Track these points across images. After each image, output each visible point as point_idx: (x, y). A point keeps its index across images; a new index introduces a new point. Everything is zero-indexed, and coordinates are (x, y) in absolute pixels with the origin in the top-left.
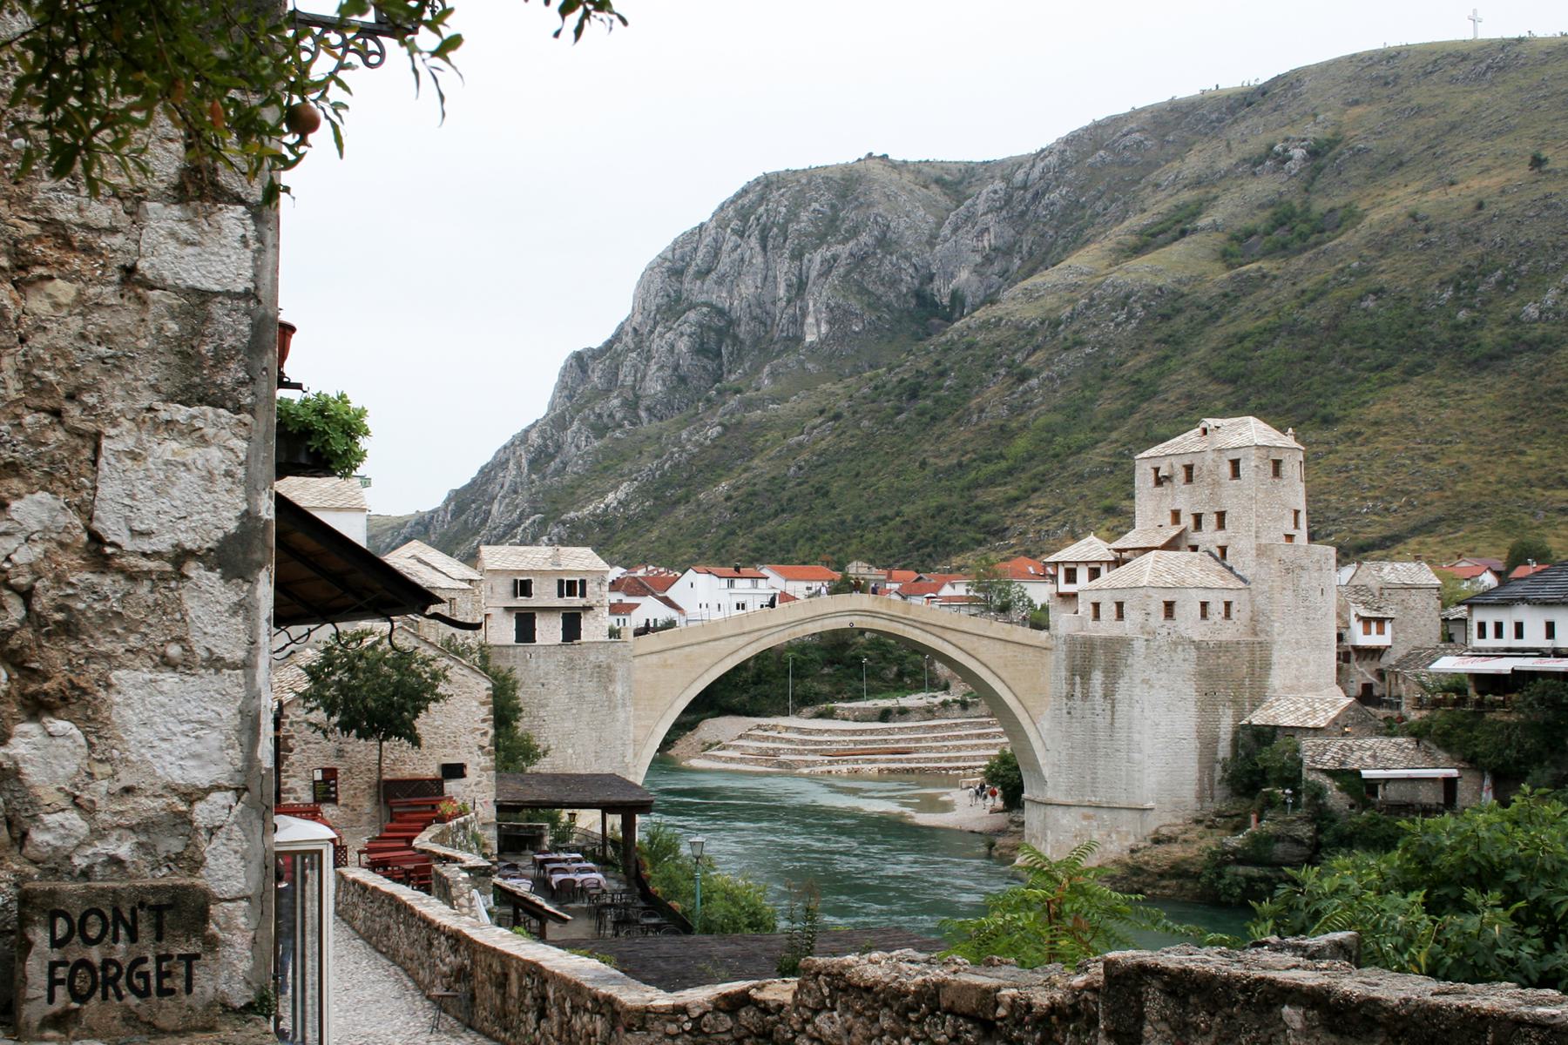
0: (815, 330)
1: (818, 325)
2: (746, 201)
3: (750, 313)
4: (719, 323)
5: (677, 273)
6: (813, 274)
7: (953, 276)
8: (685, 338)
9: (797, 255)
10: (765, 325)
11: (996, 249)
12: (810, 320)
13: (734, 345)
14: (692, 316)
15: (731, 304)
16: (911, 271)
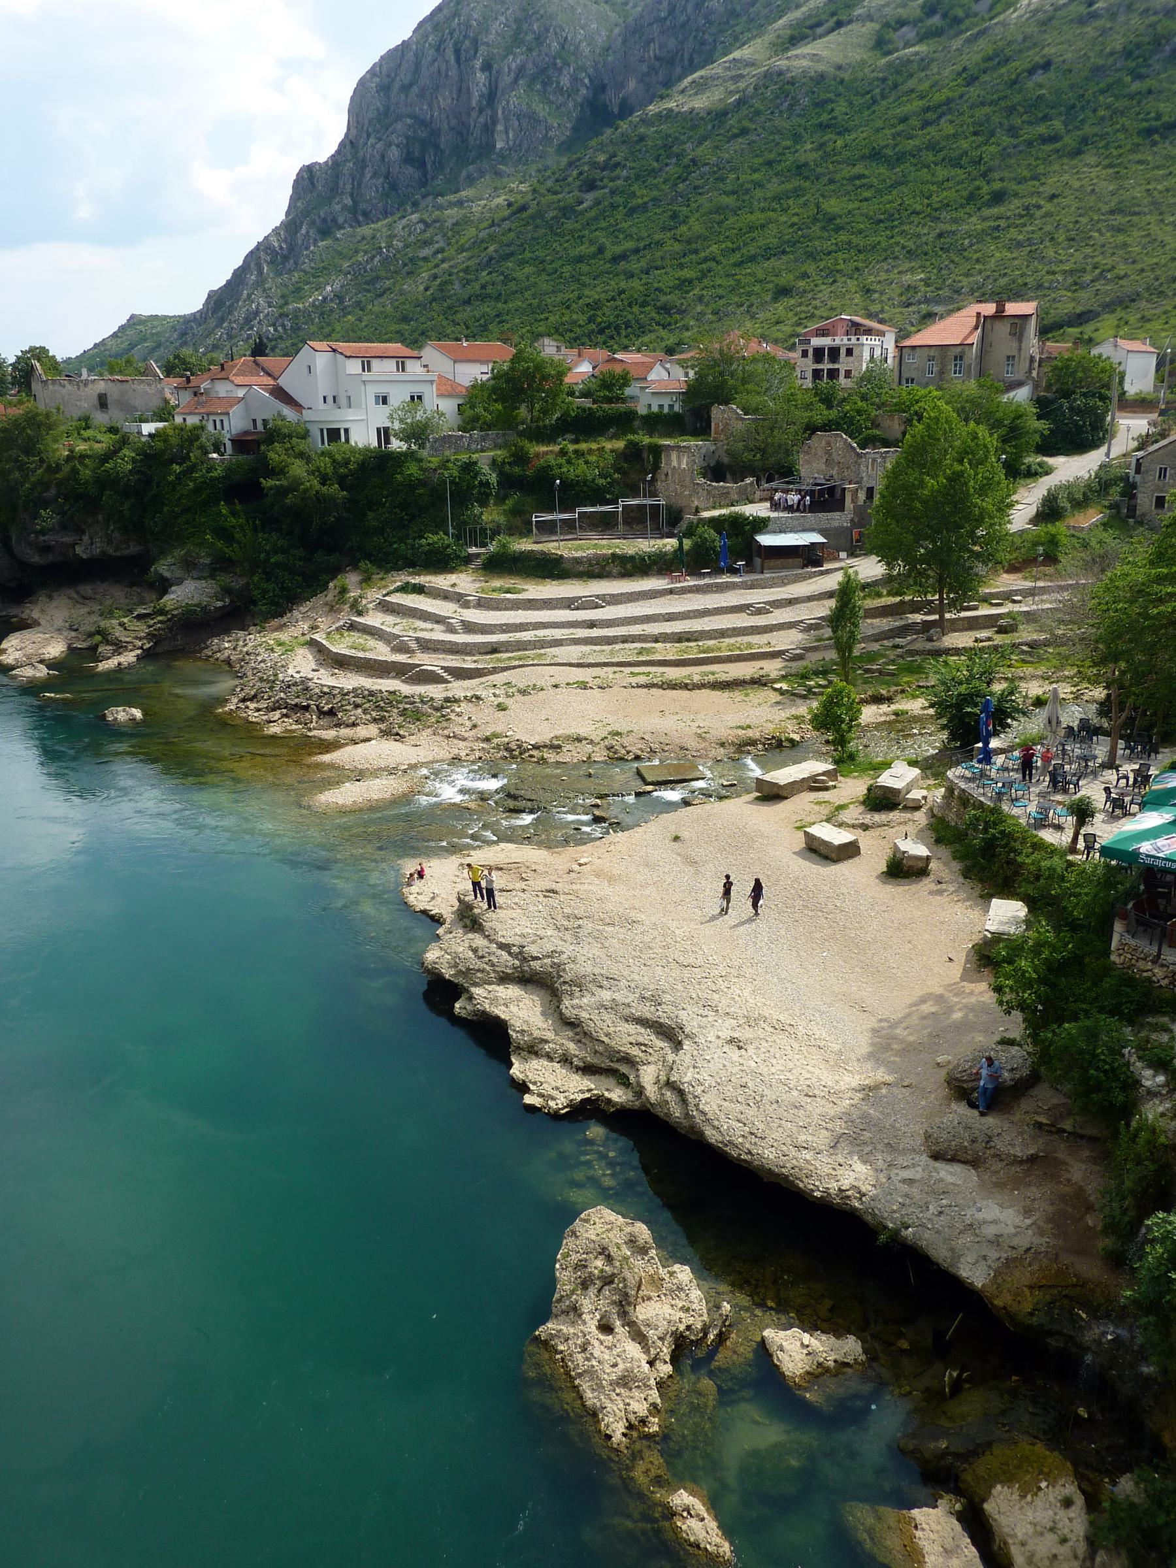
0: (504, 137)
1: (507, 132)
2: (440, 17)
3: (448, 124)
4: (423, 134)
5: (385, 88)
6: (501, 85)
7: (622, 85)
8: (394, 147)
9: (487, 67)
10: (461, 134)
11: (657, 58)
12: (500, 128)
13: (435, 155)
14: (399, 126)
15: (432, 116)
16: (586, 81)
